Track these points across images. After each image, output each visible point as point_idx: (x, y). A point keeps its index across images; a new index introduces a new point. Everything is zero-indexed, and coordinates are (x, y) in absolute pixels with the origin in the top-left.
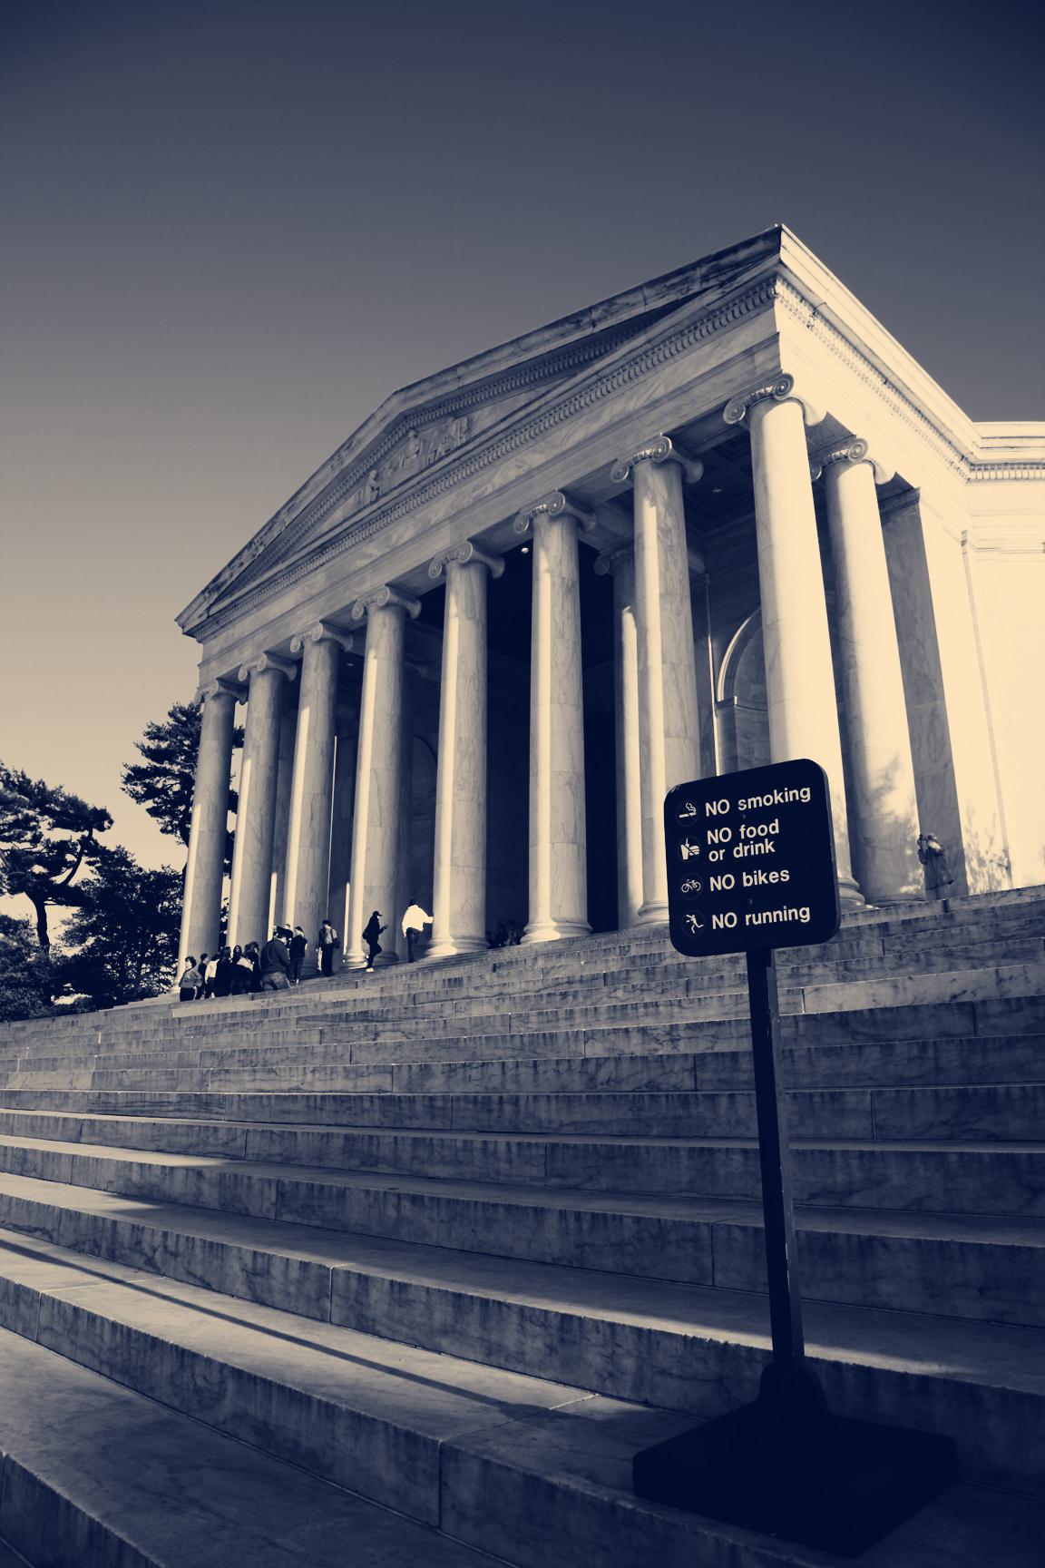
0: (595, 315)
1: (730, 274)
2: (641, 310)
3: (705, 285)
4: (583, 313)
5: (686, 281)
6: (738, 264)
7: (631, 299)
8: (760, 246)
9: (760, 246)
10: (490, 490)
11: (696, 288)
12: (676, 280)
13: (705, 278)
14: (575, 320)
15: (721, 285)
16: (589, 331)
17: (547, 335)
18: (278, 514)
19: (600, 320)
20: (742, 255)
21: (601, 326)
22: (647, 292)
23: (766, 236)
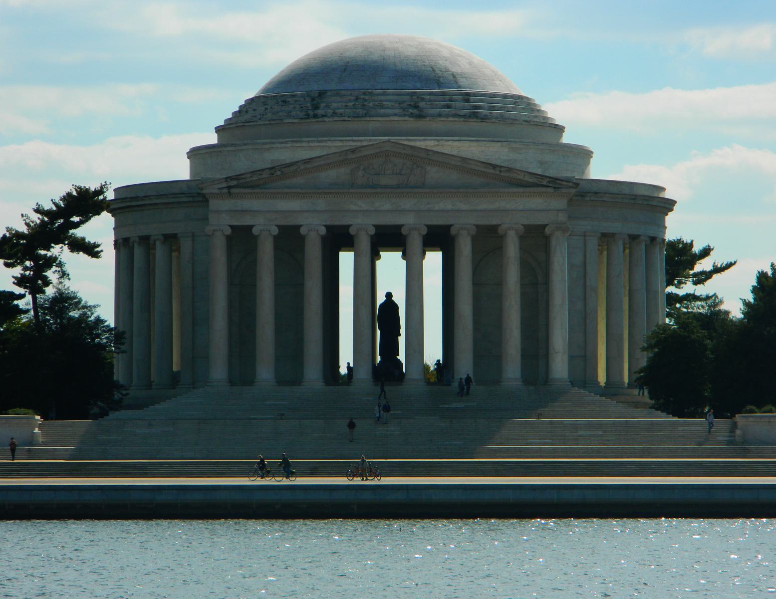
0: (502, 169)
1: (557, 186)
2: (521, 177)
3: (548, 184)
4: (497, 166)
5: (543, 179)
6: (562, 185)
7: (519, 172)
8: (571, 184)
9: (571, 184)
10: (437, 208)
11: (545, 183)
12: (538, 177)
13: (549, 182)
14: (494, 166)
15: (555, 188)
16: (498, 173)
17: (479, 164)
18: (298, 162)
19: (504, 171)
20: (564, 183)
21: (502, 174)
22: (526, 174)
23: (574, 183)
